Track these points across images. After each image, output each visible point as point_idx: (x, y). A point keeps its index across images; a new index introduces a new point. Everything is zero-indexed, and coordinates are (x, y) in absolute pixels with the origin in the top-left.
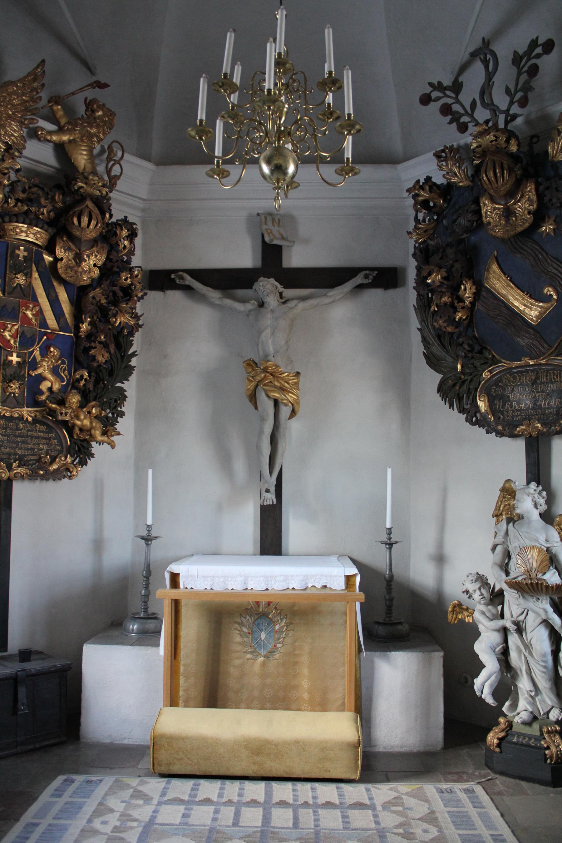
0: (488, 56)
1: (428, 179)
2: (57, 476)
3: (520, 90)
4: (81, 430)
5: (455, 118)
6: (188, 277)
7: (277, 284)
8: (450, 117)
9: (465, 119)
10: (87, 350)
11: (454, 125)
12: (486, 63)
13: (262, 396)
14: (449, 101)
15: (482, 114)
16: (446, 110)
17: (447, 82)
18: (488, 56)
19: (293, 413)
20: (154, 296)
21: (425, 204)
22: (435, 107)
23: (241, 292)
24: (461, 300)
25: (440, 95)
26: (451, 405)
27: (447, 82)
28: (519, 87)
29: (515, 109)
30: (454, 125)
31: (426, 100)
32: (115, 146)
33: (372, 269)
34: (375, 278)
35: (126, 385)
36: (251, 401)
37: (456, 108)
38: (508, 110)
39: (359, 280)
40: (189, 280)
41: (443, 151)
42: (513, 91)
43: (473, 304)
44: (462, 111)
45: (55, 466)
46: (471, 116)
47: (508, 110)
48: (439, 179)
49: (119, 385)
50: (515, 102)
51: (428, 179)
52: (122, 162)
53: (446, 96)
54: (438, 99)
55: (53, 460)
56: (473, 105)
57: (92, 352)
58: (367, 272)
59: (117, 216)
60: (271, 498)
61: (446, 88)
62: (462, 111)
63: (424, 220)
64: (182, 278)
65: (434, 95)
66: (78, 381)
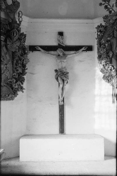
1: (101, 24)
2: (9, 99)
4: (15, 89)
6: (39, 48)
7: (62, 50)
10: (16, 68)
13: (59, 78)
14: (107, 5)
16: (106, 7)
19: (67, 82)
20: (31, 52)
21: (100, 31)
22: (103, 6)
23: (52, 52)
24: (109, 56)
25: (104, 3)
26: (106, 81)
31: (101, 4)
32: (20, 12)
33: (87, 46)
34: (87, 49)
35: (25, 77)
36: (56, 80)
37: (109, 6)
39: (83, 49)
40: (40, 49)
41: (105, 17)
43: (112, 57)
44: (110, 8)
45: (9, 97)
48: (104, 24)
49: (23, 77)
51: (101, 24)
52: (22, 17)
54: (104, 4)
55: (9, 96)
57: (17, 69)
59: (22, 32)
60: (62, 103)
62: (110, 8)
63: (100, 35)
64: (38, 48)
66: (14, 76)
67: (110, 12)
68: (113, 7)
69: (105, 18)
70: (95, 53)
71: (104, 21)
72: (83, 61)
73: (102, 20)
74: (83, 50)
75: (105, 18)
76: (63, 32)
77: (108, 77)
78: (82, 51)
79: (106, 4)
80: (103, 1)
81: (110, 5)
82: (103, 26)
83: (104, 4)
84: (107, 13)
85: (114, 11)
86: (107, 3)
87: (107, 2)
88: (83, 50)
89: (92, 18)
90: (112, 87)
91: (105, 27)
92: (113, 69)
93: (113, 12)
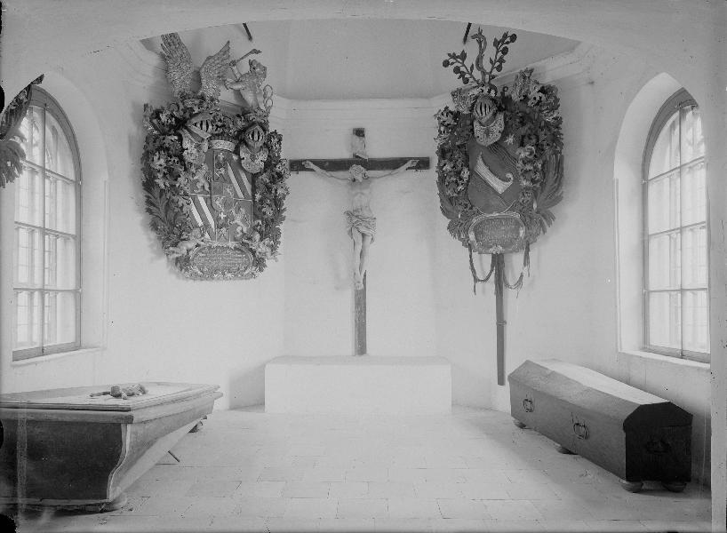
14: (459, 65)
15: (477, 74)
16: (457, 70)
22: (451, 68)
24: (461, 179)
27: (458, 54)
31: (446, 64)
39: (409, 164)
43: (468, 181)
46: (471, 74)
48: (452, 108)
54: (453, 63)
61: (457, 57)
65: (451, 61)
67: (466, 81)
68: (472, 70)
69: (456, 94)
70: (432, 175)
74: (409, 168)
75: (456, 94)
76: (428, 158)
82: (452, 113)
83: (453, 63)
84: (459, 84)
88: (409, 168)
89: (428, 97)
93: (471, 80)
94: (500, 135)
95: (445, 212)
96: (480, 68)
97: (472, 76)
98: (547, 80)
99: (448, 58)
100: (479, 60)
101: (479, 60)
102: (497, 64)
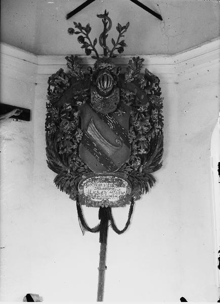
0: (107, 20)
3: (119, 44)
5: (85, 45)
8: (83, 44)
9: (90, 48)
11: (84, 49)
12: (105, 24)
14: (84, 36)
15: (99, 49)
16: (81, 39)
17: (84, 25)
18: (107, 20)
25: (80, 31)
27: (84, 25)
28: (119, 42)
29: (116, 52)
30: (84, 49)
31: (71, 31)
37: (86, 40)
38: (112, 51)
39: (13, 113)
42: (116, 42)
44: (89, 43)
46: (93, 47)
47: (112, 51)
48: (66, 70)
50: (117, 48)
53: (82, 32)
54: (77, 33)
56: (95, 41)
58: (19, 110)
61: (83, 28)
62: (89, 43)
63: (54, 91)
65: (77, 30)
68: (95, 44)
69: (73, 60)
71: (69, 67)
72: (10, 140)
73: (66, 62)
74: (13, 117)
77: (70, 181)
78: (10, 117)
79: (81, 34)
80: (76, 27)
81: (89, 39)
83: (77, 33)
85: (96, 52)
86: (84, 34)
87: (84, 31)
90: (75, 202)
91: (71, 79)
92: (83, 166)
94: (115, 106)
95: (53, 167)
96: (103, 44)
97: (94, 49)
98: (151, 69)
99: (73, 26)
100: (104, 36)
101: (104, 36)
102: (119, 46)
